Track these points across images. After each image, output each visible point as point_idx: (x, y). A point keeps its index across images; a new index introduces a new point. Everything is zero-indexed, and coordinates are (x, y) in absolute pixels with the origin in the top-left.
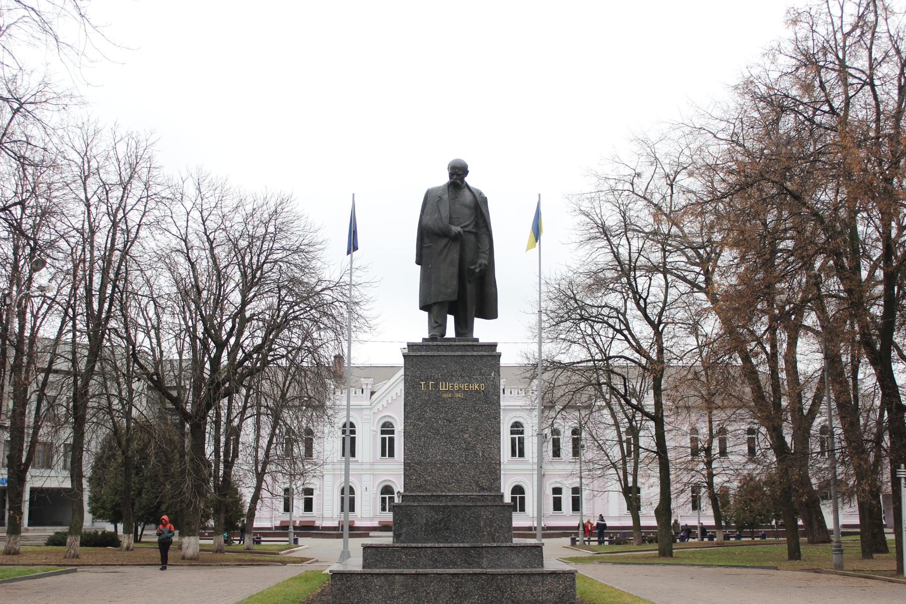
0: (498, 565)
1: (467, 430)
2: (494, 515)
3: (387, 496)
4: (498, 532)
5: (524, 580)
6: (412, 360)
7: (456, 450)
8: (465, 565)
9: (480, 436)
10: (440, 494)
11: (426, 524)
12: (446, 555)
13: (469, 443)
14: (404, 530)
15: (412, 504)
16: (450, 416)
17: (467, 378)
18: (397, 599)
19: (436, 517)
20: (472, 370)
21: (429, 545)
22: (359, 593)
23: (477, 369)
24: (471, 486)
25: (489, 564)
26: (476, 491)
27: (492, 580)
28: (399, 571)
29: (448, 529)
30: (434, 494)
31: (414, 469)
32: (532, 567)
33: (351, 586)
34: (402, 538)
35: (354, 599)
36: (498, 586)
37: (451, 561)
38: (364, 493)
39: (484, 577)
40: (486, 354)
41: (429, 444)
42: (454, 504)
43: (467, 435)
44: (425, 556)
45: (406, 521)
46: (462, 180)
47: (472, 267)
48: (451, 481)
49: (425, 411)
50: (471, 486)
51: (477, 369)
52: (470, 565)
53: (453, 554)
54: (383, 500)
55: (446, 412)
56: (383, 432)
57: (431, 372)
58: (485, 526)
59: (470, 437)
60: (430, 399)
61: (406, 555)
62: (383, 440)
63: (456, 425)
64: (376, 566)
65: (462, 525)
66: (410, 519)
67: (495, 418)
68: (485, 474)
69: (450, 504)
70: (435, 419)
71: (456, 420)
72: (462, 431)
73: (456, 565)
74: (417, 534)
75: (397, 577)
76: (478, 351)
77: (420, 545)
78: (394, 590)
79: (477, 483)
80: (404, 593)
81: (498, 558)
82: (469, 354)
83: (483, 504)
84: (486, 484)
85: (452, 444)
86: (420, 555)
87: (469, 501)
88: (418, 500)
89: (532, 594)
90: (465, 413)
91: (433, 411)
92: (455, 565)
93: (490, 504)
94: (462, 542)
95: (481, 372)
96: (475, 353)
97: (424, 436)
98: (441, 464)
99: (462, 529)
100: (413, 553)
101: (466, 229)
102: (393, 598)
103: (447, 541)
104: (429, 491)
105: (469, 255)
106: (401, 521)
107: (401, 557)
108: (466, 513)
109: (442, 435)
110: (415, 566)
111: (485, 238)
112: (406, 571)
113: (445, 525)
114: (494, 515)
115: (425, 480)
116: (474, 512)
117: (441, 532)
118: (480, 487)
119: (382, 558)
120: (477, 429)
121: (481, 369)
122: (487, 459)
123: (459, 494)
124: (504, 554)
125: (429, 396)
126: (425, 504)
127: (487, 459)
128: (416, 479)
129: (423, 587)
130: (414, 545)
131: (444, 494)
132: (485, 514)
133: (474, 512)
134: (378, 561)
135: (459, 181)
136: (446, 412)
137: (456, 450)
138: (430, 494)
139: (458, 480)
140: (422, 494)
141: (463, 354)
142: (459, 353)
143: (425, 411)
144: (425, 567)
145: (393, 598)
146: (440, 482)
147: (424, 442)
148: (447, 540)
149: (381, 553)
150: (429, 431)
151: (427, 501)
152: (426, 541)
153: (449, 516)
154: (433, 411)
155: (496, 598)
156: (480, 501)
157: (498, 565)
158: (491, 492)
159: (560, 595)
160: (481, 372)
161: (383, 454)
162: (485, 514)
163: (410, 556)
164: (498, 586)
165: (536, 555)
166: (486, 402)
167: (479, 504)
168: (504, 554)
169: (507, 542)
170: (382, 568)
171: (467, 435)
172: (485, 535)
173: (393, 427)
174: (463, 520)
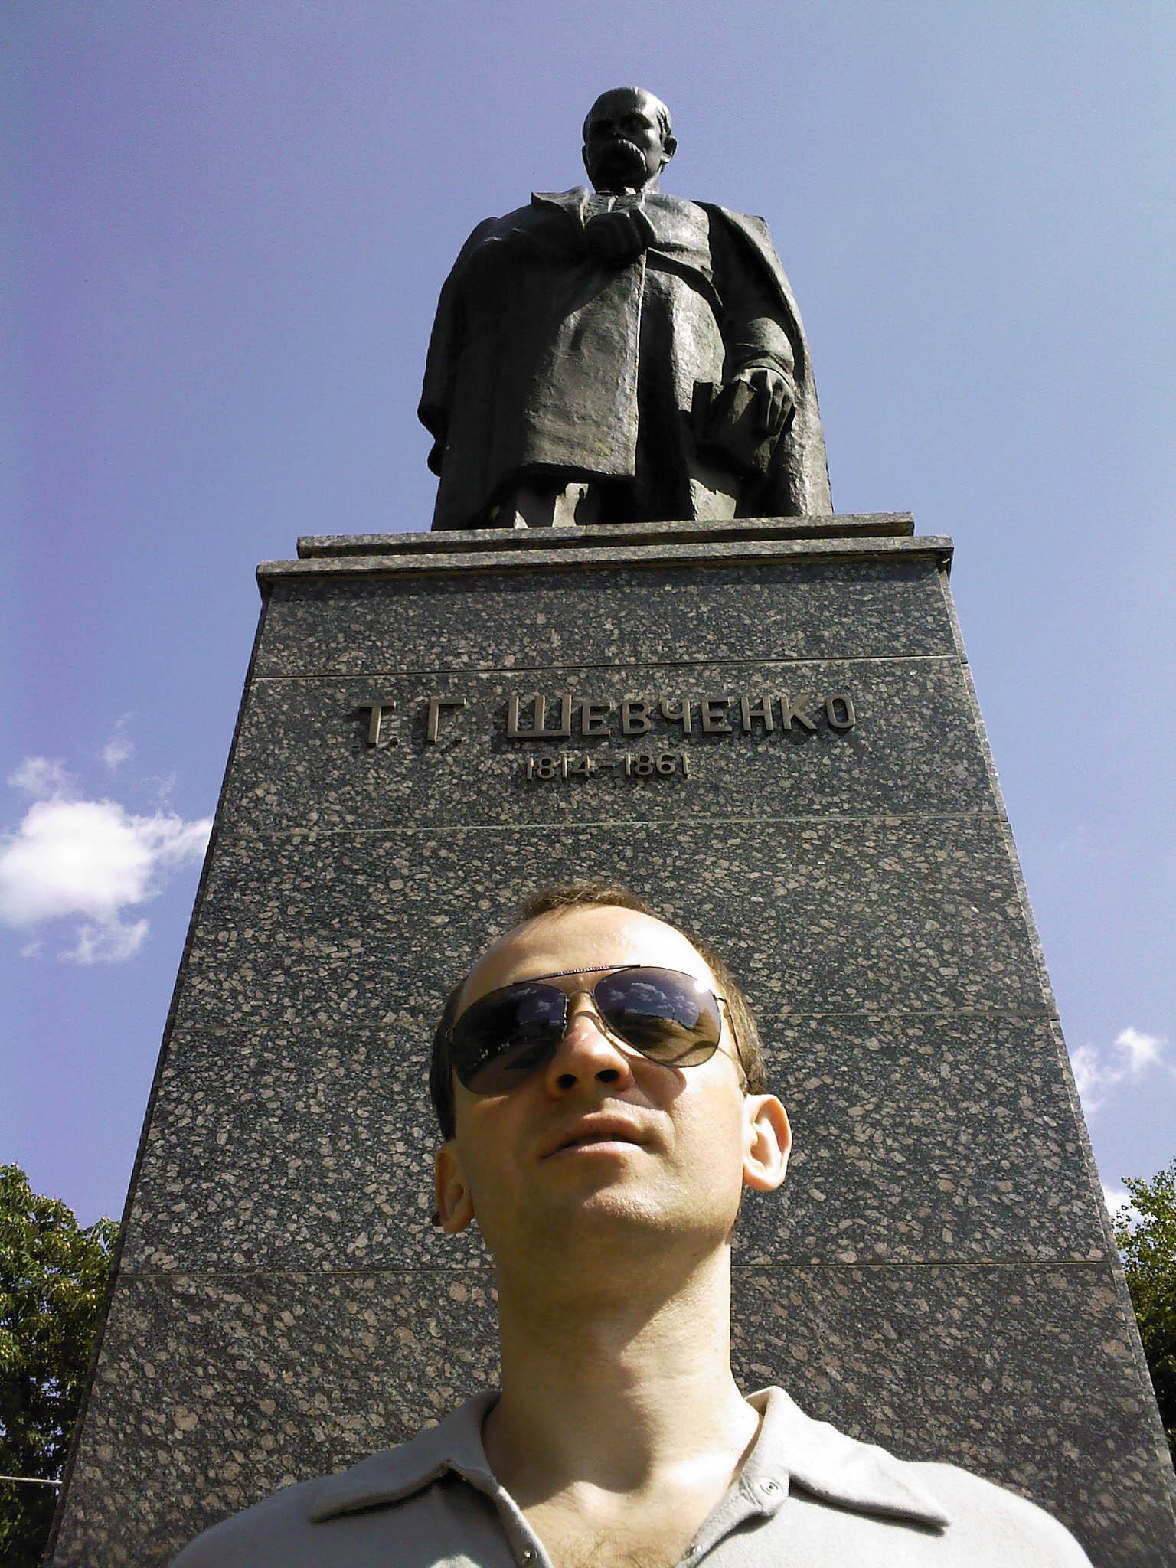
9: (860, 1026)
31: (207, 1337)
49: (371, 870)
68: (974, 1373)
70: (455, 917)
91: (445, 866)
95: (815, 640)
97: (346, 1042)
120: (827, 978)
122: (963, 1225)
125: (422, 775)
127: (963, 1225)
128: (193, 1440)
143: (371, 870)
150: (394, 1005)
154: (445, 866)
160: (815, 640)
166: (887, 800)
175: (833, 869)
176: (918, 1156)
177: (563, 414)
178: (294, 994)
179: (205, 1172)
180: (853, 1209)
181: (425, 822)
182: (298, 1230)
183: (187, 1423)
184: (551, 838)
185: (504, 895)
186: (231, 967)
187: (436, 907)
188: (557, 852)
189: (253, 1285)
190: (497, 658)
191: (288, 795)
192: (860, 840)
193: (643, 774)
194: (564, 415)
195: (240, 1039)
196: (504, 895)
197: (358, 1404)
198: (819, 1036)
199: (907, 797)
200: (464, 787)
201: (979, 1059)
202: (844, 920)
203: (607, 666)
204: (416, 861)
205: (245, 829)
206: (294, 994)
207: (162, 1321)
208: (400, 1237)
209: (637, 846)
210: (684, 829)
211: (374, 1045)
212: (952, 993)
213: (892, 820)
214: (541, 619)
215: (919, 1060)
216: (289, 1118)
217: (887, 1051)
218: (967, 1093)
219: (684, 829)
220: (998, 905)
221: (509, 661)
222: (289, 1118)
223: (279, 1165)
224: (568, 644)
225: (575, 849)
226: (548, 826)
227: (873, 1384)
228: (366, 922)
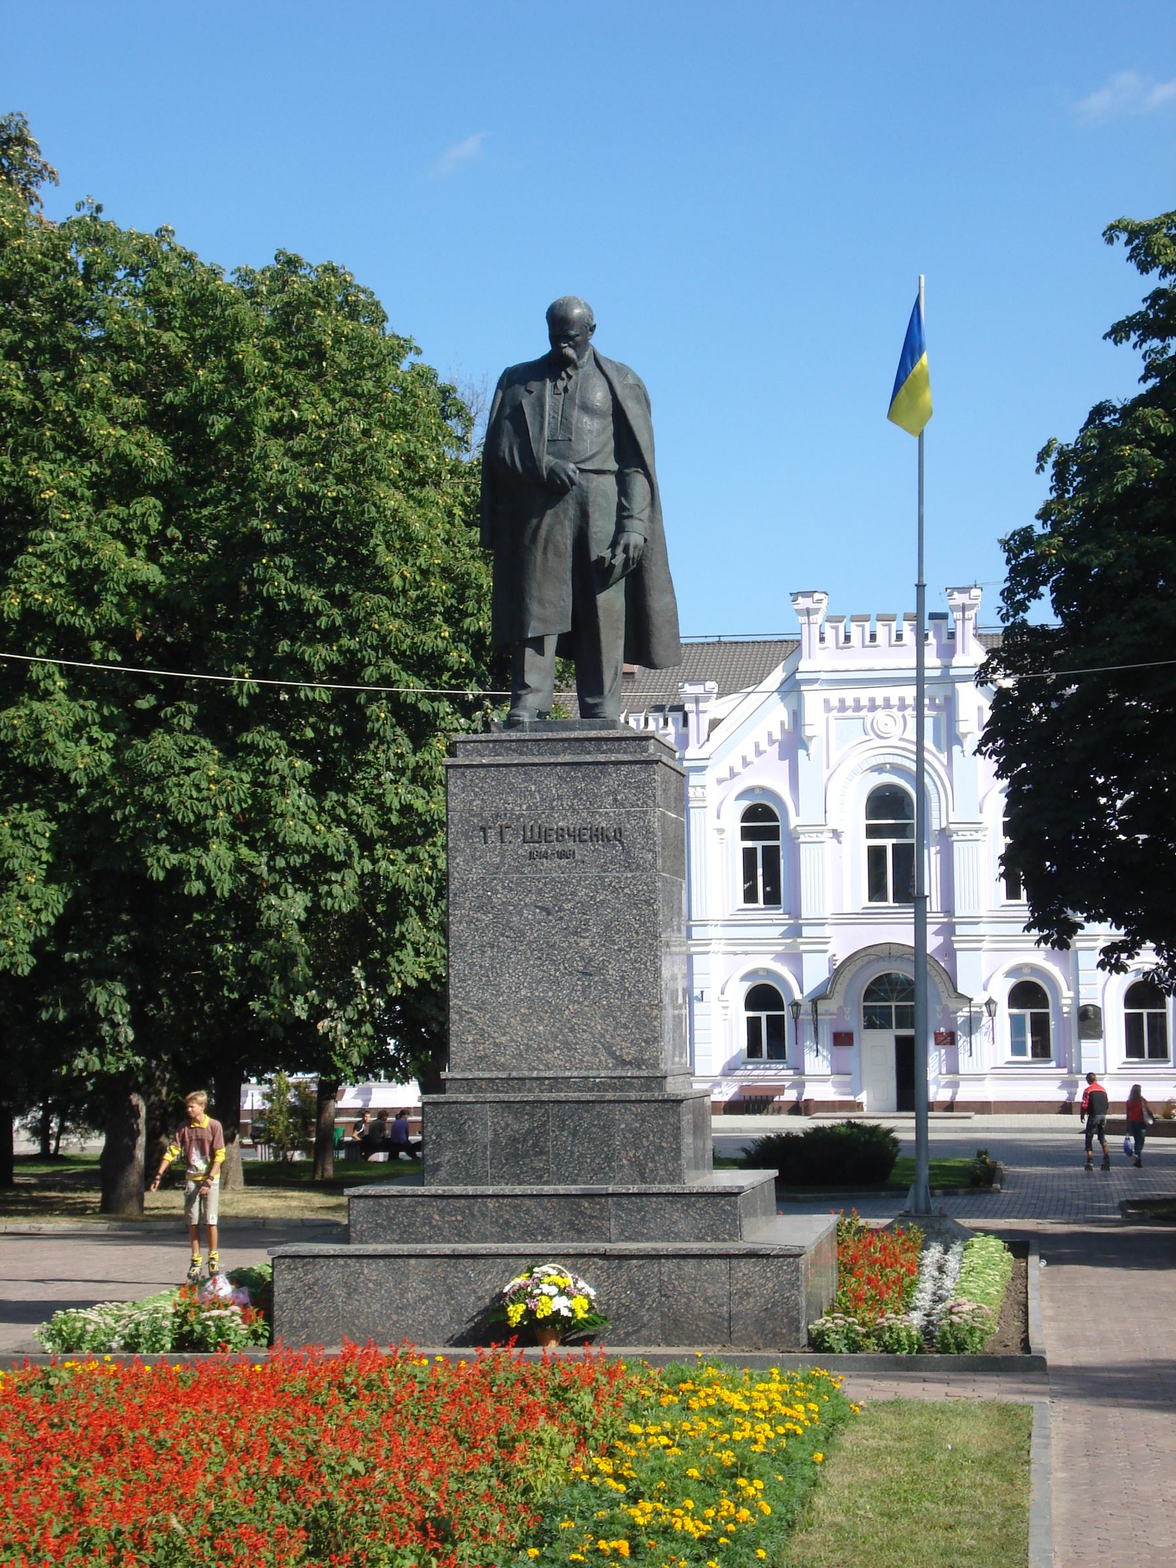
0: (643, 1235)
1: (587, 930)
2: (643, 1120)
3: (763, 1015)
4: (653, 1160)
5: (689, 1266)
6: (463, 773)
7: (563, 975)
8: (571, 1234)
10: (526, 1074)
11: (495, 1143)
12: (528, 1211)
13: (591, 960)
14: (448, 1155)
15: (462, 1098)
16: (548, 901)
17: (584, 814)
18: (414, 1309)
19: (516, 1127)
20: (596, 796)
21: (490, 1190)
22: (333, 1297)
23: (608, 794)
24: (595, 1055)
25: (622, 1233)
26: (607, 1068)
27: (620, 1267)
28: (418, 1248)
29: (541, 1153)
30: (514, 1074)
31: (471, 1020)
32: (717, 1239)
33: (315, 1284)
34: (442, 1174)
35: (321, 1311)
36: (631, 1281)
37: (541, 1225)
38: (696, 1005)
39: (601, 1262)
40: (626, 758)
41: (502, 963)
42: (554, 1096)
43: (587, 942)
44: (483, 1214)
45: (449, 1137)
46: (581, 346)
47: (607, 554)
48: (551, 1046)
50: (595, 1055)
51: (608, 794)
52: (580, 1233)
53: (545, 1209)
54: (753, 1024)
55: (540, 892)
56: (747, 834)
57: (506, 802)
58: (624, 1147)
59: (592, 945)
60: (502, 863)
61: (441, 1212)
62: (749, 855)
63: (561, 918)
64: (376, 1239)
65: (573, 1145)
66: (460, 1132)
67: (647, 902)
68: (627, 1028)
69: (545, 1096)
70: (515, 907)
71: (561, 909)
72: (576, 933)
73: (551, 1234)
74: (475, 1165)
75: (413, 1261)
76: (611, 751)
77: (470, 1190)
78: (406, 1290)
79: (608, 1049)
80: (428, 1298)
81: (643, 1218)
82: (589, 758)
83: (618, 1095)
84: (630, 1053)
85: (553, 962)
86: (472, 1214)
87: (591, 1090)
88: (480, 1090)
89: (706, 1301)
90: (582, 893)
91: (511, 890)
92: (548, 1234)
93: (633, 1095)
94: (574, 1182)
95: (616, 800)
96: (601, 758)
97: (492, 947)
98: (530, 1008)
99: (572, 1152)
100: (456, 1209)
101: (582, 466)
102: (405, 1307)
103: (539, 1180)
104: (503, 1067)
105: (602, 526)
106: (439, 1136)
107: (430, 1218)
108: (581, 1118)
109: (530, 942)
110: (463, 1237)
111: (639, 483)
112: (431, 1248)
113: (535, 1145)
114: (643, 1120)
115: (496, 1045)
116: (599, 1114)
117: (527, 1161)
118: (616, 1058)
119: (390, 1219)
120: (607, 928)
121: (614, 793)
122: (630, 995)
123: (568, 1074)
124: (656, 1211)
125: (502, 855)
126: (490, 1096)
127: (630, 995)
128: (473, 1042)
129: (469, 1283)
130: (458, 1189)
131: (535, 1074)
132: (623, 1120)
133: (599, 1114)
134: (381, 1226)
135: (570, 352)
136: (540, 892)
137: (563, 975)
138: (504, 1075)
139: (566, 1043)
140: (487, 1075)
141: (577, 759)
142: (568, 758)
144: (484, 1239)
145: (405, 1307)
146: (528, 1047)
147: (492, 959)
148: (542, 1177)
149: (388, 1208)
150: (502, 935)
151: (498, 1091)
152: (495, 1180)
153: (544, 1124)
154: (511, 890)
155: (628, 1308)
156: (615, 1089)
157: (643, 1235)
158: (640, 1068)
159: (767, 1302)
160: (616, 800)
161: (750, 896)
162: (623, 1120)
163: (449, 1214)
164: (631, 1281)
165: (725, 1212)
166: (628, 868)
167: (610, 1096)
168: (656, 1211)
169: (673, 1182)
170: (390, 1242)
171: (587, 942)
172: (623, 1166)
173: (776, 819)
174: (574, 1133)
175: (612, 892)
176: (623, 978)
177: (541, 602)
178: (477, 930)
179: (464, 981)
180: (607, 991)
181: (505, 873)
182: (487, 995)
183: (470, 1039)
184: (539, 880)
185: (527, 900)
186: (460, 922)
187: (509, 904)
188: (541, 885)
189: (480, 1009)
190: (521, 806)
191: (466, 862)
192: (620, 882)
193: (562, 855)
194: (541, 602)
195: (466, 944)
196: (527, 900)
197: (504, 1034)
198: (604, 945)
199: (634, 866)
200: (514, 859)
201: (640, 952)
202: (613, 910)
203: (553, 808)
204: (504, 888)
205: (456, 875)
206: (477, 930)
207: (461, 1017)
208: (510, 998)
209: (561, 882)
210: (574, 878)
211: (499, 947)
212: (637, 933)
213: (629, 875)
214: (533, 788)
215: (627, 952)
216: (481, 967)
217: (619, 950)
218: (636, 961)
219: (574, 878)
220: (651, 905)
221: (524, 807)
222: (481, 967)
223: (481, 980)
224: (542, 800)
225: (545, 884)
226: (538, 876)
227: (607, 1031)
228: (492, 908)
